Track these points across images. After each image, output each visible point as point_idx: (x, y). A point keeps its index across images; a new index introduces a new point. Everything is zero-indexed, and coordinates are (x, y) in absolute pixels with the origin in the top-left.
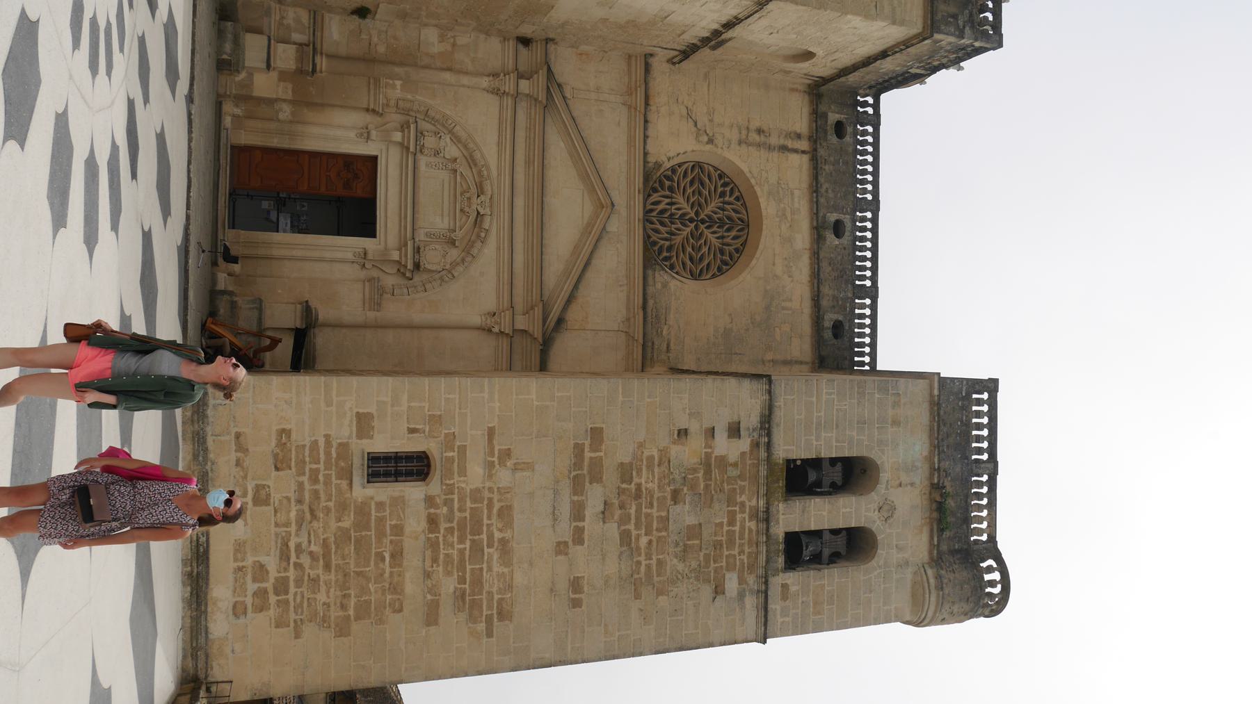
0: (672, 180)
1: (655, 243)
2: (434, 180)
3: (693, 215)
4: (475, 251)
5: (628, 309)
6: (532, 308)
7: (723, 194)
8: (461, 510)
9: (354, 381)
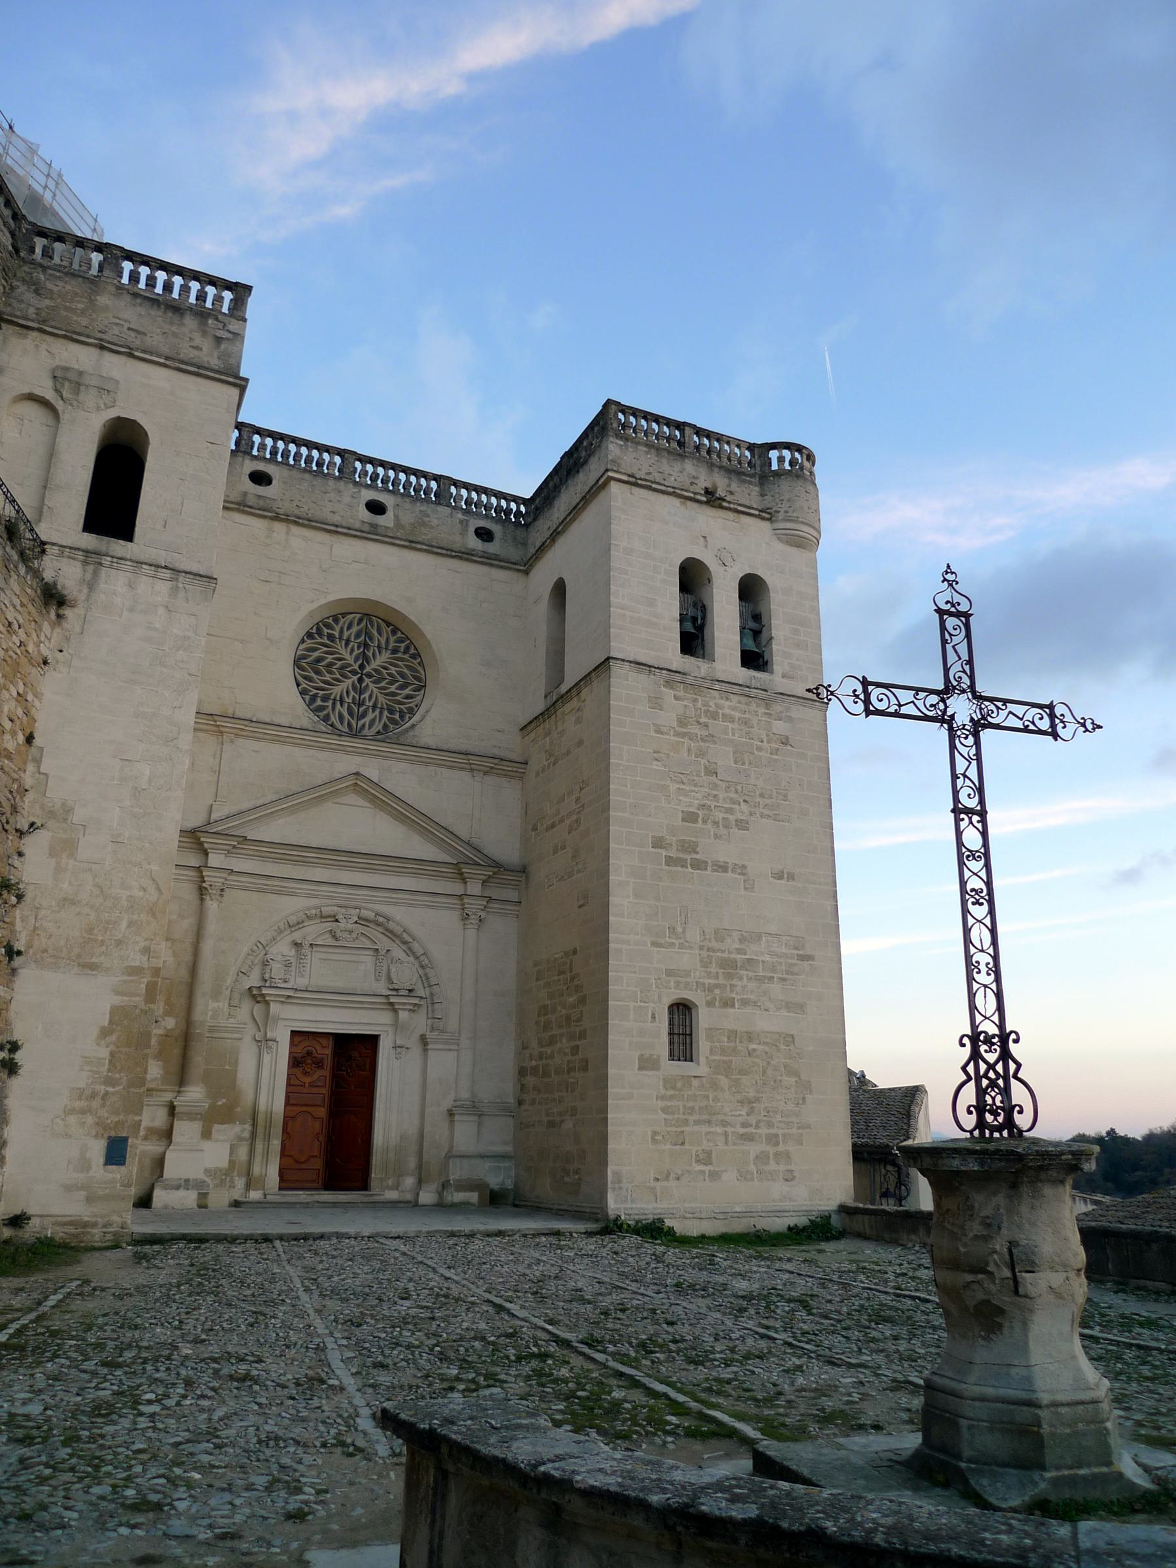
0: (316, 696)
1: (385, 727)
2: (321, 971)
3: (355, 678)
4: (398, 930)
5: (461, 769)
6: (462, 874)
7: (331, 637)
8: (717, 977)
9: (612, 1071)
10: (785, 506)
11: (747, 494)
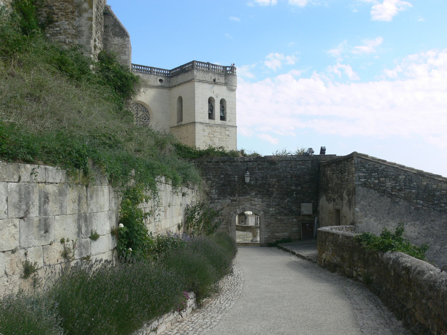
10: (230, 82)
11: (222, 80)
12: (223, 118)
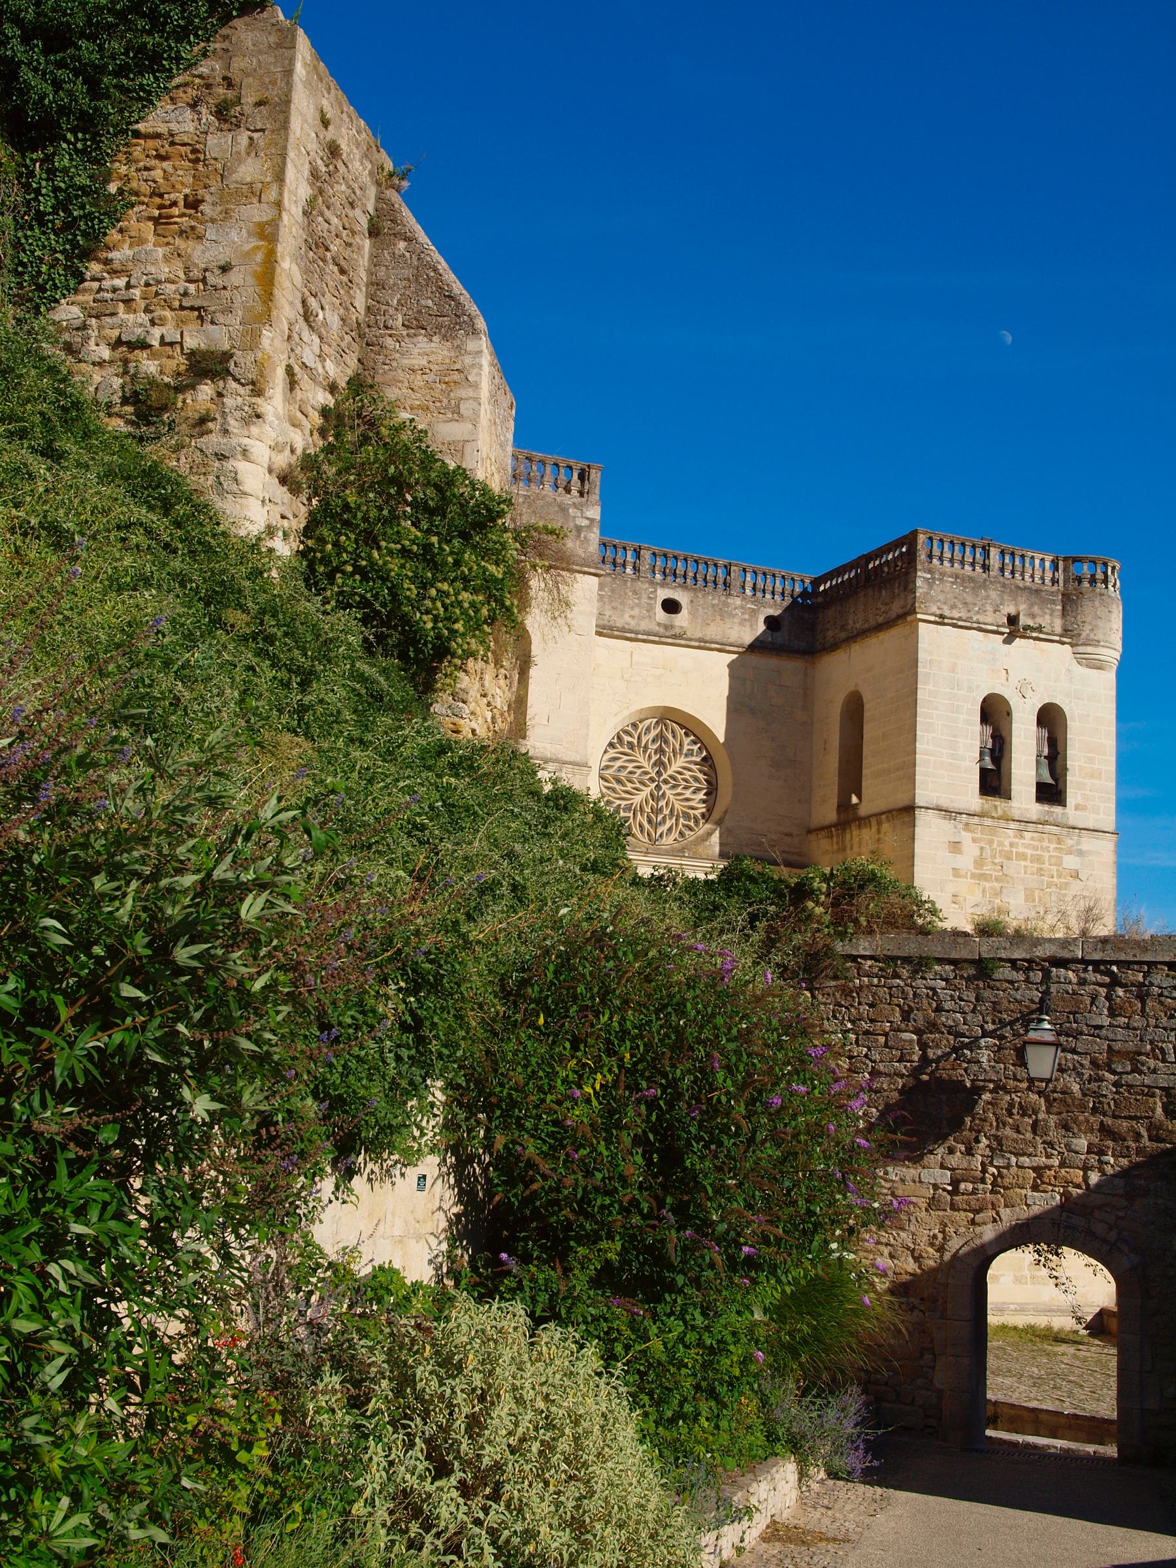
10: (1087, 628)
12: (1051, 792)
